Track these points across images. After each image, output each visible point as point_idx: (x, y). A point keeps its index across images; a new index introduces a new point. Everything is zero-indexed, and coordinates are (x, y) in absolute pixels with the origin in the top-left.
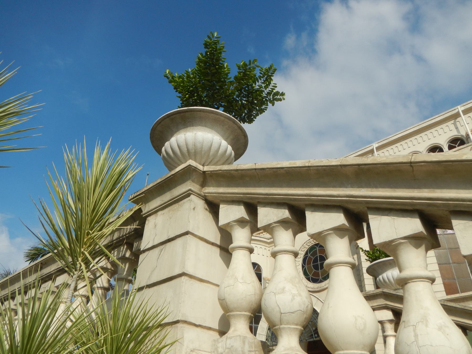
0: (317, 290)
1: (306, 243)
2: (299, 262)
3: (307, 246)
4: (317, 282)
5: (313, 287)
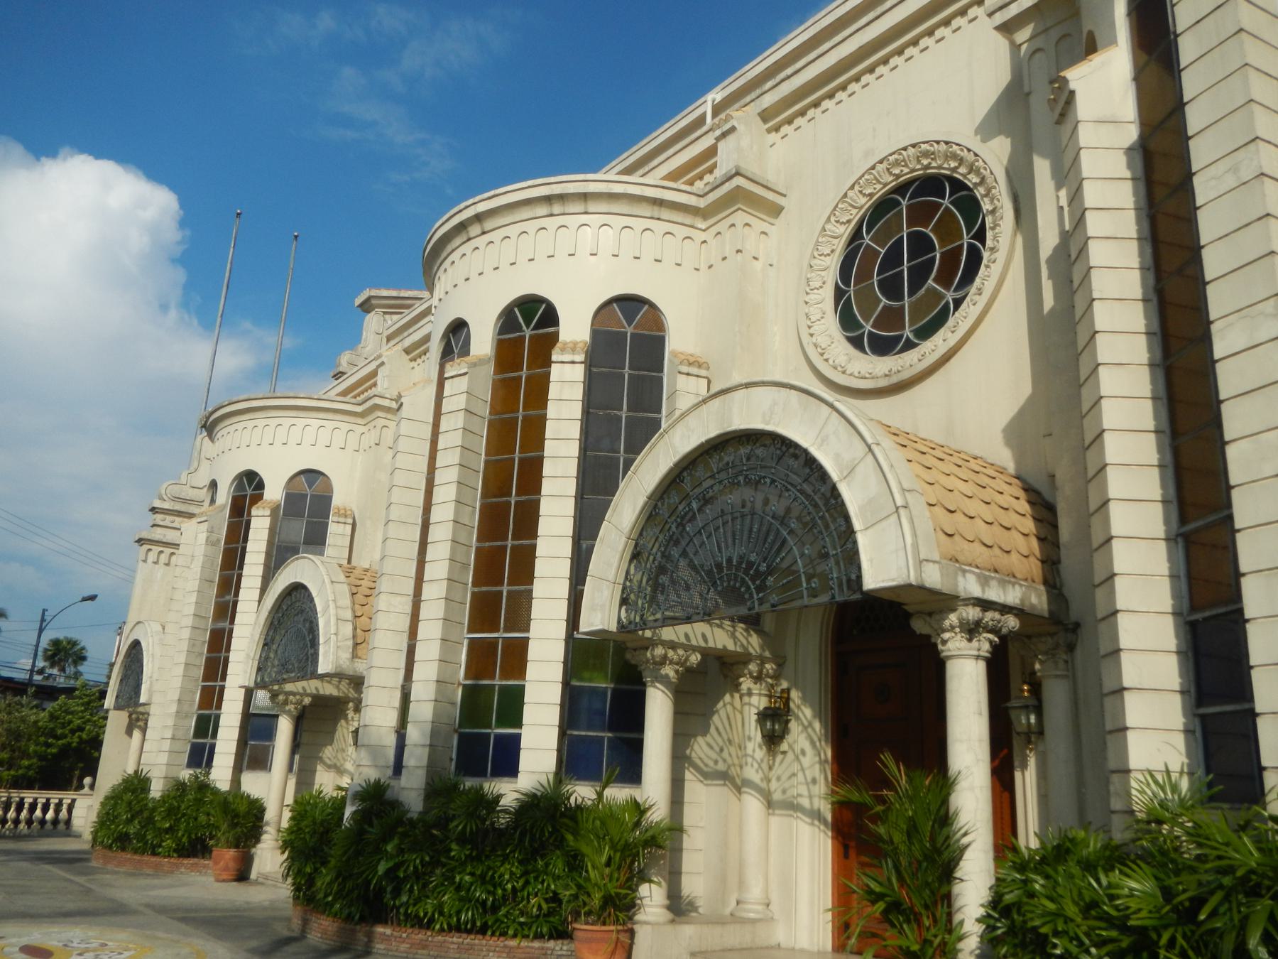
0: (882, 383)
1: (857, 187)
2: (823, 273)
3: (863, 200)
4: (894, 349)
5: (870, 374)
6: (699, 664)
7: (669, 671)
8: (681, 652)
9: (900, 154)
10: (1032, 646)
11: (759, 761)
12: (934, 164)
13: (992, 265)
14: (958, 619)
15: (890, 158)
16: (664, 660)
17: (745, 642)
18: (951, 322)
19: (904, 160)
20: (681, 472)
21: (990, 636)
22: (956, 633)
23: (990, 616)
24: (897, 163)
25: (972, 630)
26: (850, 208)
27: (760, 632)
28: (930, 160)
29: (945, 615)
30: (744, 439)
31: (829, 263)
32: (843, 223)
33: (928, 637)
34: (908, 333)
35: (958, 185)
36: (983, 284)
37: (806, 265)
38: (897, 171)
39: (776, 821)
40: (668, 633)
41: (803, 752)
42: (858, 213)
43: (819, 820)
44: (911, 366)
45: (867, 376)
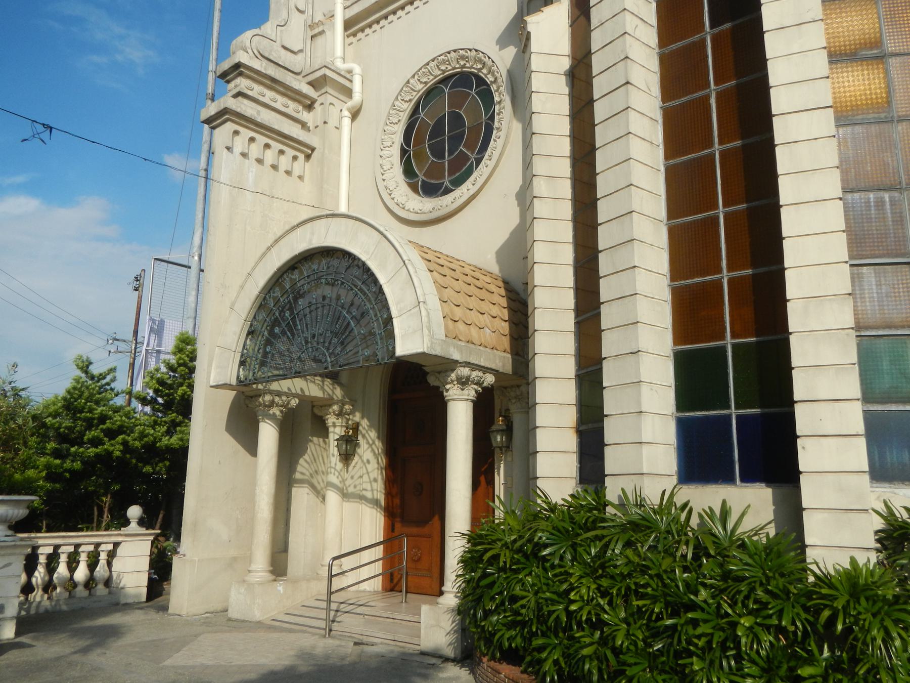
1: (416, 77)
3: (420, 86)
5: (421, 210)
6: (298, 406)
7: (276, 411)
8: (284, 398)
9: (446, 56)
10: (507, 394)
11: (339, 470)
12: (468, 65)
13: (498, 140)
14: (456, 375)
15: (439, 58)
16: (272, 404)
17: (330, 392)
18: (472, 179)
19: (448, 61)
20: (281, 276)
21: (476, 387)
22: (454, 385)
23: (476, 374)
24: (443, 62)
25: (463, 382)
26: (411, 91)
27: (340, 385)
28: (465, 62)
29: (448, 373)
30: (325, 253)
31: (396, 129)
32: (407, 102)
33: (438, 388)
34: (447, 182)
35: (481, 81)
36: (492, 153)
37: (381, 130)
38: (443, 68)
39: (350, 507)
40: (275, 386)
41: (368, 462)
42: (417, 95)
43: (377, 506)
44: (447, 206)
45: (419, 211)
